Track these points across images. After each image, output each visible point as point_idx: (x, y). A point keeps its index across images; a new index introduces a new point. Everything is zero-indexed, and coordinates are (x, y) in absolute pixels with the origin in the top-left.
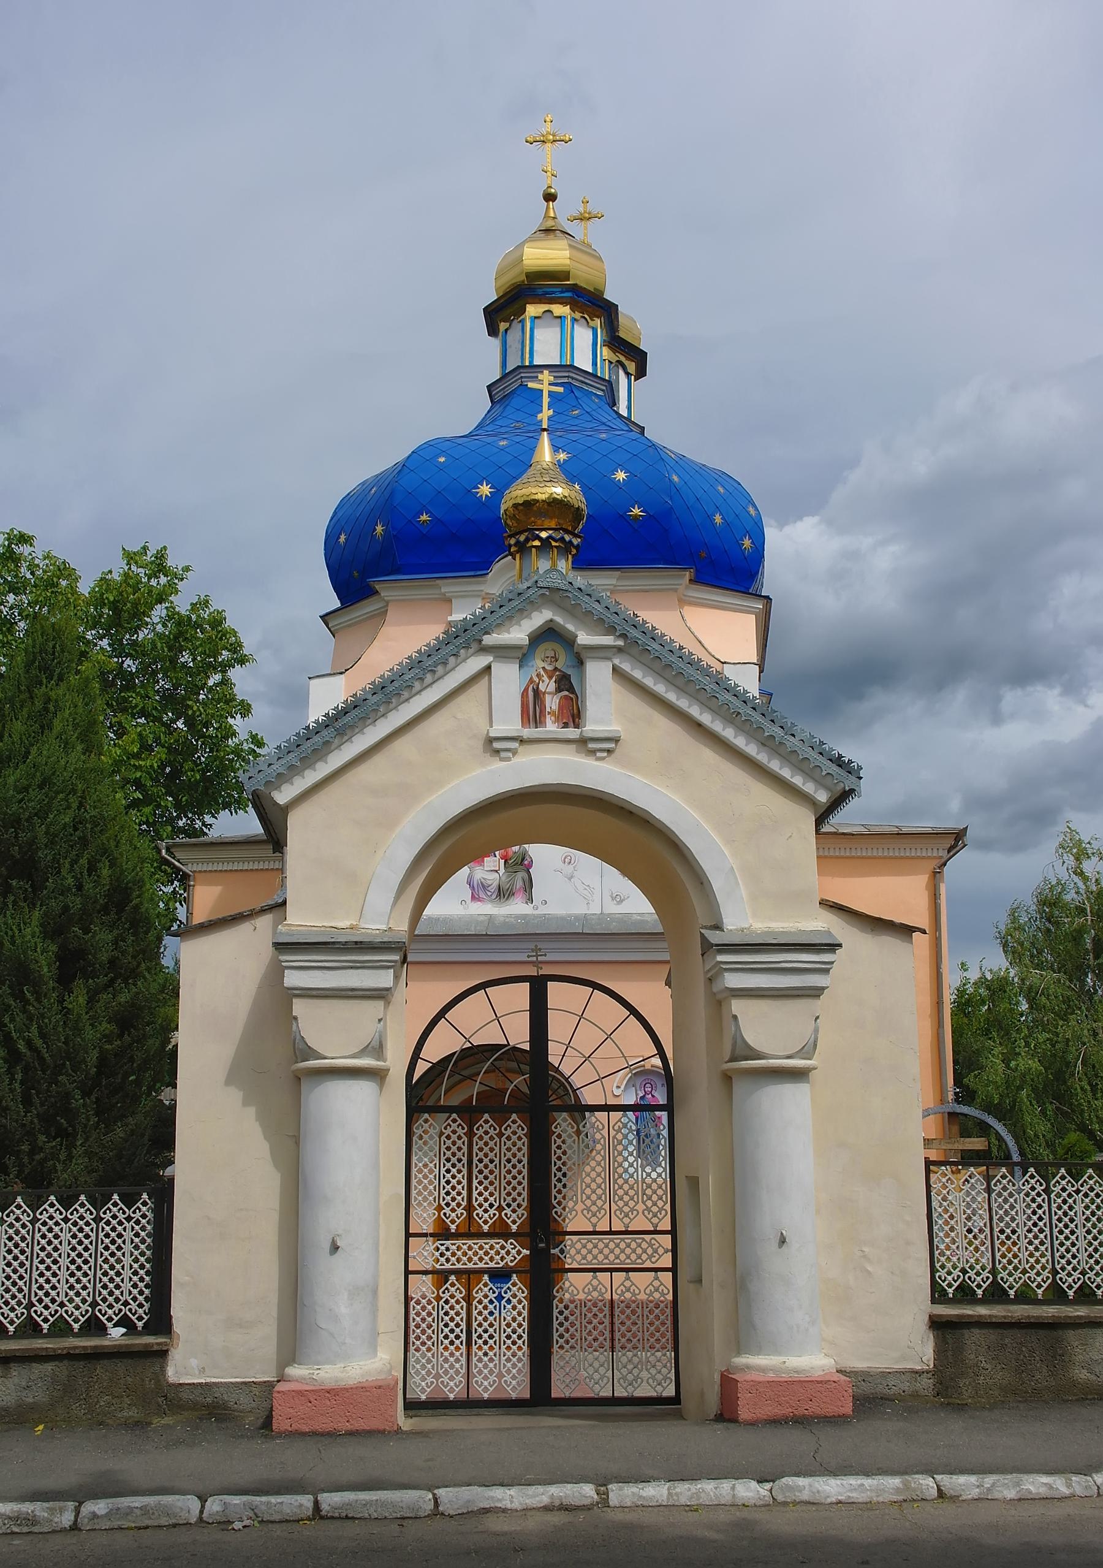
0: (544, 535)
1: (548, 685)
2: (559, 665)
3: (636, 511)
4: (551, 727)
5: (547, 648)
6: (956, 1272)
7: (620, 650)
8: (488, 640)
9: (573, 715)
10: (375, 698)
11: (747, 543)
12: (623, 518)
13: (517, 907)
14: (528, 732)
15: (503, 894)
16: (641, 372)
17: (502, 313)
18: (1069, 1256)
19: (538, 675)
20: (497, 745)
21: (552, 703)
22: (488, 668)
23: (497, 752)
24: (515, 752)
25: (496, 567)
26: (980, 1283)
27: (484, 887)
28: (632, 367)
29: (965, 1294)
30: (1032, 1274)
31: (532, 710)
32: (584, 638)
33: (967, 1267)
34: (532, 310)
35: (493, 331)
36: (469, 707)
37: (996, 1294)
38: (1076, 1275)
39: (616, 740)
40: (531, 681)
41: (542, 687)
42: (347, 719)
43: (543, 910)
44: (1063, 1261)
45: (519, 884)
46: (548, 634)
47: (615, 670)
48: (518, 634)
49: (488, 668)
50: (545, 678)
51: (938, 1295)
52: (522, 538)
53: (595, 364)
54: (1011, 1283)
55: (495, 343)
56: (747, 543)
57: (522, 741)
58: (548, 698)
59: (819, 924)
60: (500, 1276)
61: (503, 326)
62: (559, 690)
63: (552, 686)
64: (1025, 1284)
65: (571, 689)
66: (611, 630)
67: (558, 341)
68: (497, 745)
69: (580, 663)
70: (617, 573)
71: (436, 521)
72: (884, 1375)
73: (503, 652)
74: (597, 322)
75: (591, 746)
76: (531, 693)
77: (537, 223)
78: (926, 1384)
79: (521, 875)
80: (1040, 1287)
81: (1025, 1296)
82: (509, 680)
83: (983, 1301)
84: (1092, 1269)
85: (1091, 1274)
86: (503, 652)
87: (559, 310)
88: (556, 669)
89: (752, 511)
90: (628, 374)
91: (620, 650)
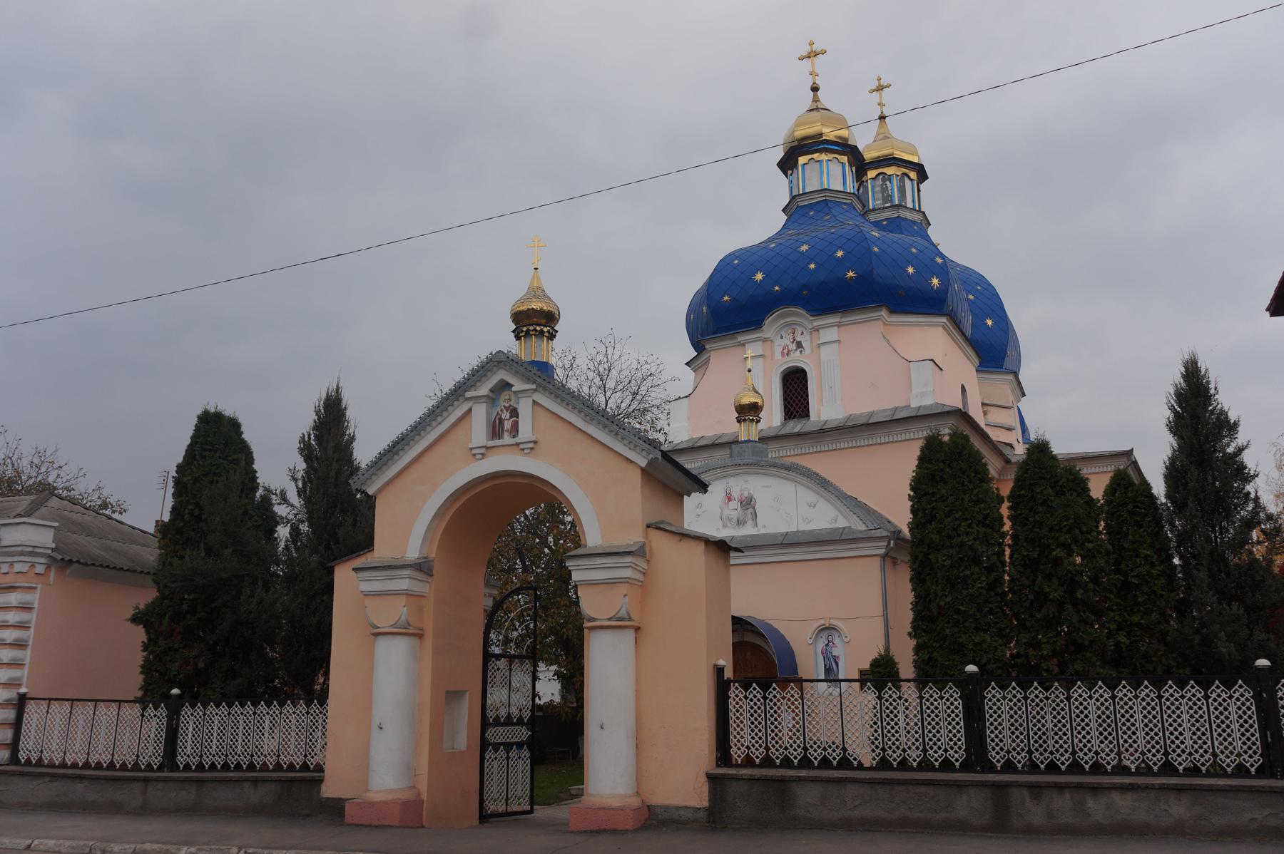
1: (506, 415)
4: (507, 439)
5: (505, 395)
6: (743, 749)
7: (535, 390)
8: (468, 395)
9: (515, 430)
11: (935, 281)
12: (843, 279)
14: (497, 442)
15: (740, 523)
17: (787, 164)
20: (474, 452)
21: (507, 425)
22: (470, 410)
25: (767, 321)
26: (758, 755)
27: (729, 519)
28: (913, 175)
31: (496, 430)
34: (802, 160)
36: (459, 433)
37: (768, 762)
39: (535, 442)
43: (763, 531)
45: (749, 516)
48: (484, 390)
49: (470, 410)
56: (935, 281)
57: (487, 448)
60: (520, 745)
68: (474, 452)
71: (733, 300)
72: (678, 808)
77: (808, 104)
78: (703, 815)
79: (751, 510)
80: (796, 758)
82: (480, 416)
87: (815, 156)
89: (939, 260)
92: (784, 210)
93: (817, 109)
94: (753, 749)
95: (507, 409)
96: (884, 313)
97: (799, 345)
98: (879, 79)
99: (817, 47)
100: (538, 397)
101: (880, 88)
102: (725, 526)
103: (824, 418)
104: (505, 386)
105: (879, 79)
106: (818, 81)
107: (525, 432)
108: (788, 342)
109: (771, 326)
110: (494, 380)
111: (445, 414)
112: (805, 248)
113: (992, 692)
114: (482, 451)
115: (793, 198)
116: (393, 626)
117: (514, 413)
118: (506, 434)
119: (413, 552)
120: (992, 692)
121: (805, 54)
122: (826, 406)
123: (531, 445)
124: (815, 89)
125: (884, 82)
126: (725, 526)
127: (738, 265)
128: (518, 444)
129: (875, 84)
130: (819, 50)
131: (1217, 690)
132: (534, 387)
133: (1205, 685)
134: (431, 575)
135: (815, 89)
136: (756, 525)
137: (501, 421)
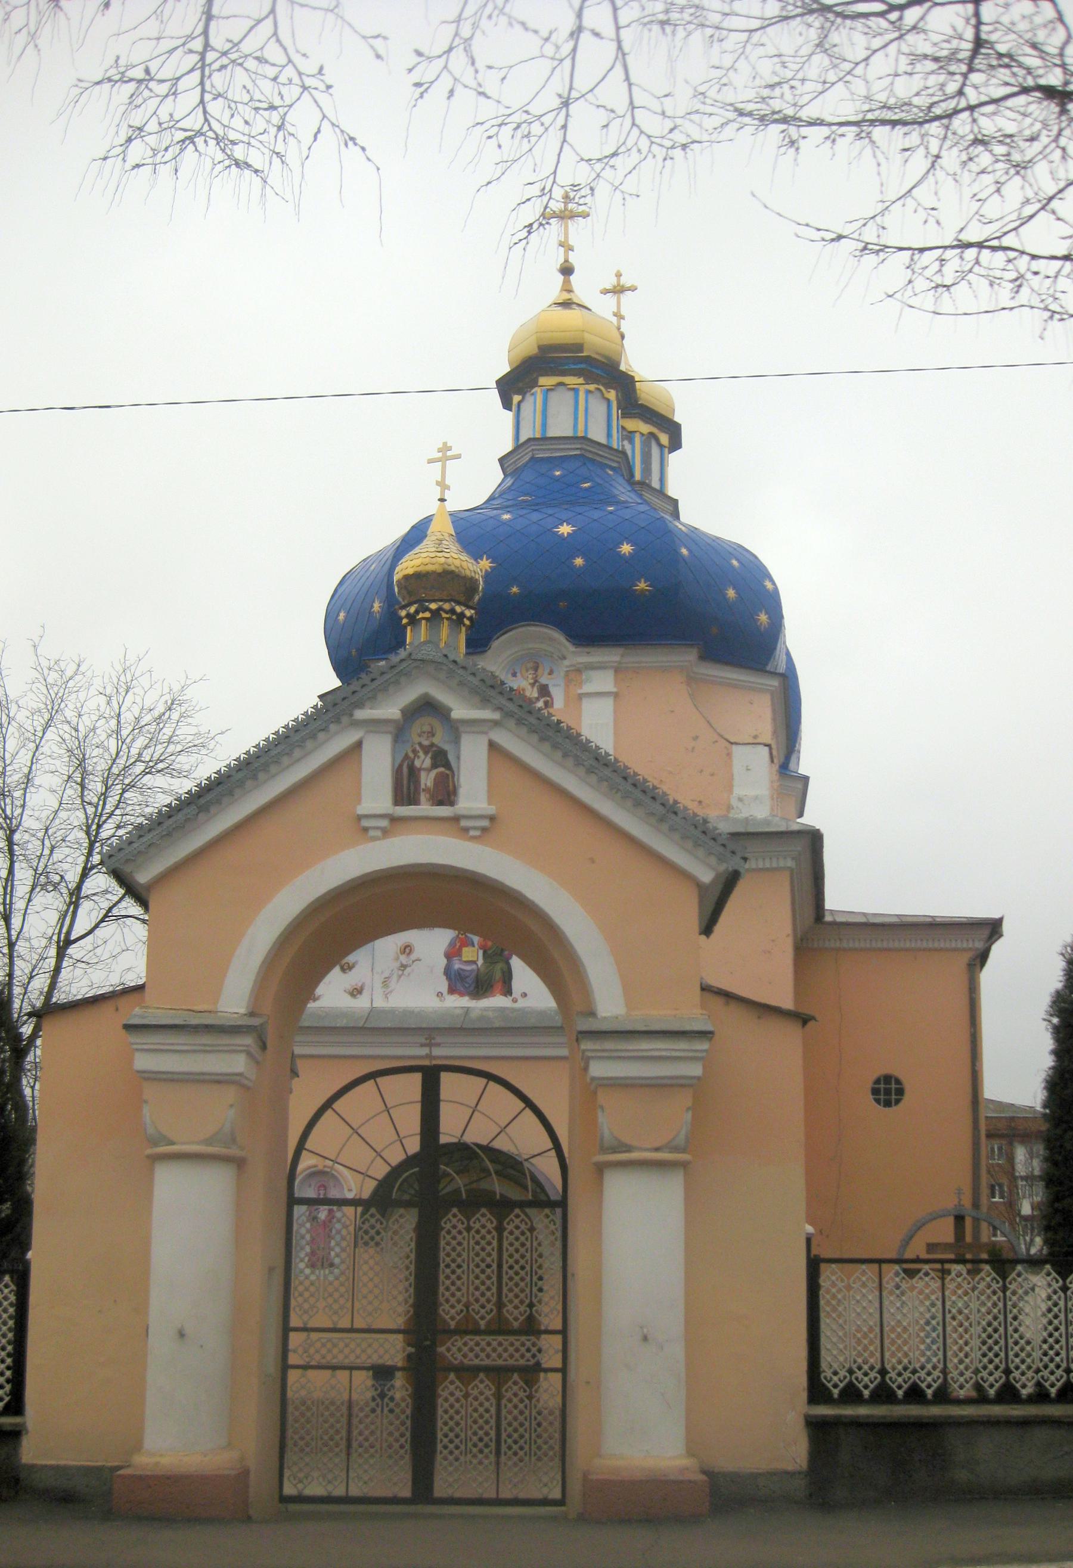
0: (433, 606)
1: (424, 761)
2: (436, 740)
5: (424, 723)
7: (496, 723)
8: (360, 714)
9: (445, 794)
10: (240, 775)
13: (497, 1001)
15: (480, 986)
16: (676, 444)
17: (514, 386)
18: (991, 1355)
19: (414, 751)
20: (365, 823)
21: (427, 780)
22: (359, 745)
23: (366, 830)
25: (495, 644)
26: (867, 1383)
28: (664, 439)
29: (851, 1394)
30: (923, 1374)
32: (460, 712)
33: (854, 1367)
35: (507, 404)
37: (883, 1394)
38: (968, 1374)
39: (492, 818)
40: (406, 757)
41: (417, 763)
42: (209, 797)
43: (522, 1003)
44: (1017, 1360)
45: (498, 975)
46: (427, 707)
47: (492, 746)
49: (359, 745)
50: (421, 754)
51: (817, 1391)
52: (412, 609)
53: (609, 435)
54: (899, 1385)
55: (509, 415)
57: (394, 819)
58: (423, 774)
59: (692, 1014)
61: (516, 398)
62: (434, 766)
63: (428, 762)
64: (851, 1383)
65: (447, 765)
66: (485, 702)
67: (573, 413)
69: (457, 741)
70: (620, 651)
73: (375, 725)
74: (612, 395)
75: (464, 823)
76: (405, 770)
79: (499, 966)
81: (982, 1398)
84: (985, 1368)
85: (984, 1374)
86: (375, 725)
87: (569, 380)
88: (432, 745)
90: (661, 446)
91: (496, 723)
92: (501, 461)
93: (567, 304)
94: (859, 1374)
95: (426, 750)
96: (689, 656)
98: (619, 275)
100: (507, 740)
101: (618, 290)
102: (452, 990)
104: (427, 707)
105: (619, 275)
106: (573, 258)
107: (474, 795)
110: (410, 694)
111: (310, 744)
114: (384, 823)
116: (208, 1142)
117: (440, 758)
118: (423, 797)
123: (485, 823)
124: (567, 270)
125: (626, 281)
126: (452, 990)
128: (456, 819)
129: (610, 282)
132: (496, 716)
135: (567, 270)
136: (508, 991)
137: (414, 773)
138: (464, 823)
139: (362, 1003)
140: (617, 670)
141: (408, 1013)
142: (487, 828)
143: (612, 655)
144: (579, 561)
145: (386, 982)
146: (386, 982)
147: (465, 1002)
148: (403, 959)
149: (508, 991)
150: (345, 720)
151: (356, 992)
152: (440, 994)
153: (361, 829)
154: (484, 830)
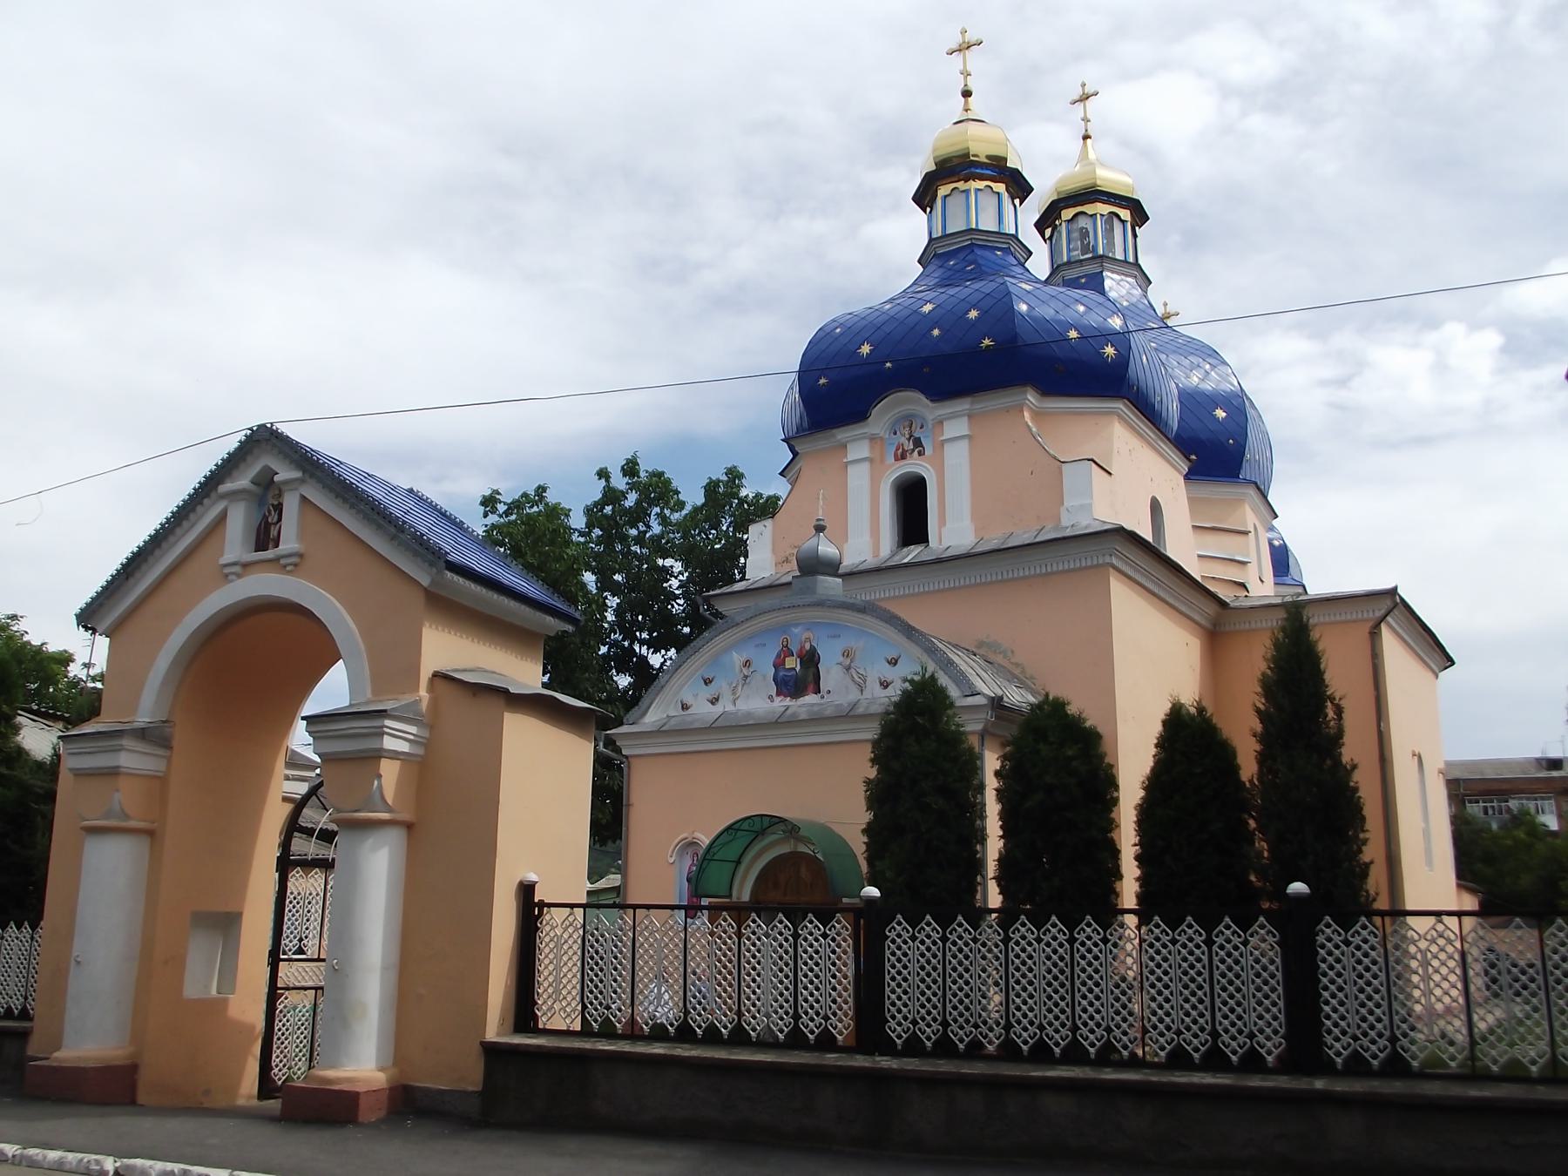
3: (987, 342)
7: (302, 481)
13: (810, 699)
17: (924, 197)
20: (227, 570)
24: (239, 576)
25: (874, 412)
28: (1125, 214)
31: (264, 537)
39: (301, 556)
45: (811, 678)
48: (242, 481)
68: (227, 570)
70: (969, 399)
73: (233, 495)
75: (283, 561)
79: (812, 670)
83: (623, 1037)
97: (918, 443)
98: (1084, 85)
99: (971, 37)
101: (1085, 98)
103: (945, 544)
105: (1084, 85)
107: (289, 541)
108: (903, 440)
109: (882, 417)
112: (928, 308)
113: (898, 929)
114: (237, 569)
115: (931, 240)
119: (143, 718)
120: (898, 929)
121: (955, 46)
122: (952, 528)
124: (967, 94)
127: (841, 334)
128: (277, 560)
129: (1077, 94)
130: (973, 40)
131: (1227, 930)
133: (1209, 924)
134: (170, 748)
135: (967, 94)
136: (818, 691)
138: (283, 561)
139: (718, 709)
140: (970, 417)
141: (749, 714)
142: (294, 564)
143: (963, 405)
144: (936, 332)
145: (734, 691)
146: (734, 691)
147: (788, 701)
148: (745, 671)
149: (818, 691)
150: (213, 495)
151: (714, 701)
152: (771, 697)
153: (226, 575)
154: (296, 565)
